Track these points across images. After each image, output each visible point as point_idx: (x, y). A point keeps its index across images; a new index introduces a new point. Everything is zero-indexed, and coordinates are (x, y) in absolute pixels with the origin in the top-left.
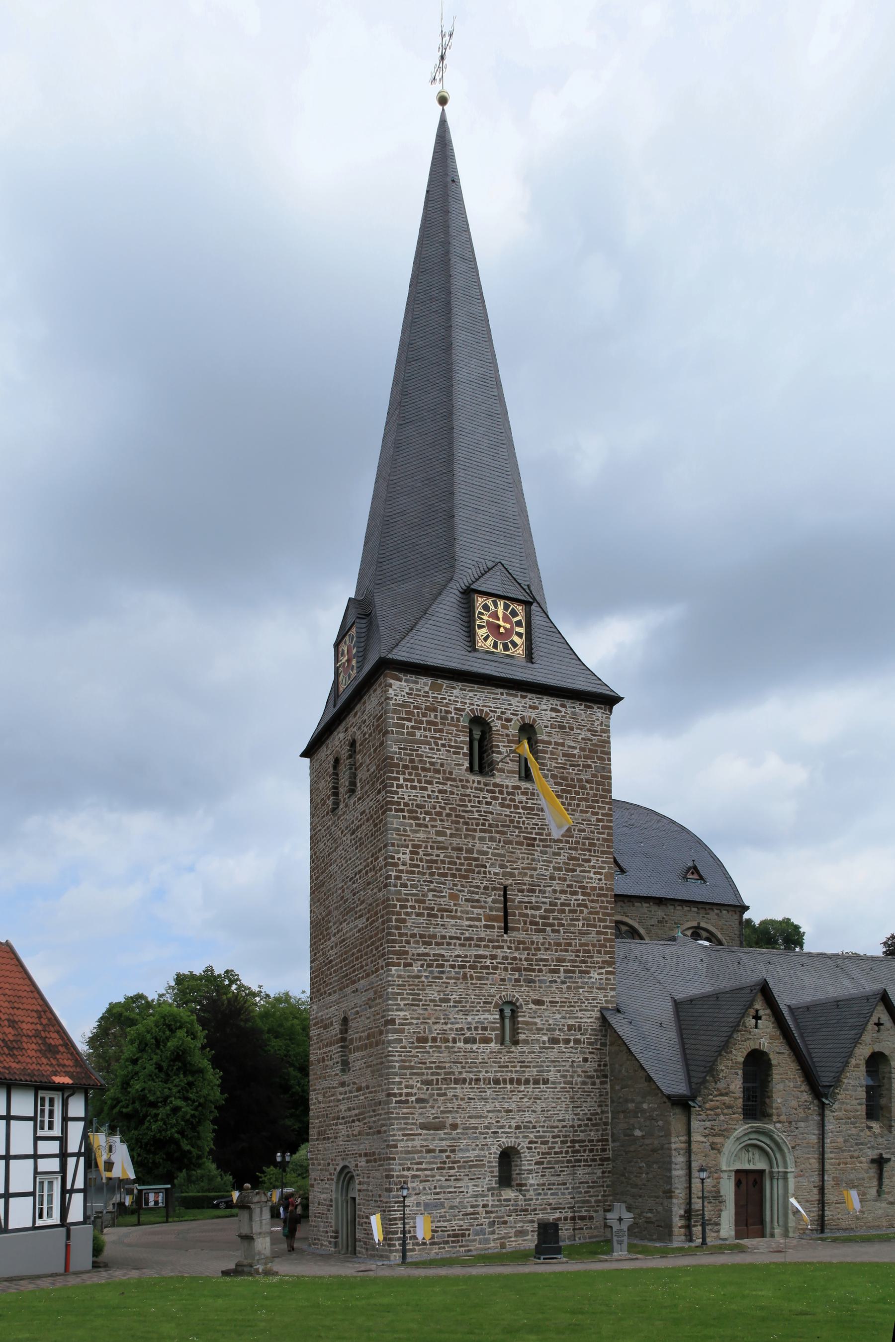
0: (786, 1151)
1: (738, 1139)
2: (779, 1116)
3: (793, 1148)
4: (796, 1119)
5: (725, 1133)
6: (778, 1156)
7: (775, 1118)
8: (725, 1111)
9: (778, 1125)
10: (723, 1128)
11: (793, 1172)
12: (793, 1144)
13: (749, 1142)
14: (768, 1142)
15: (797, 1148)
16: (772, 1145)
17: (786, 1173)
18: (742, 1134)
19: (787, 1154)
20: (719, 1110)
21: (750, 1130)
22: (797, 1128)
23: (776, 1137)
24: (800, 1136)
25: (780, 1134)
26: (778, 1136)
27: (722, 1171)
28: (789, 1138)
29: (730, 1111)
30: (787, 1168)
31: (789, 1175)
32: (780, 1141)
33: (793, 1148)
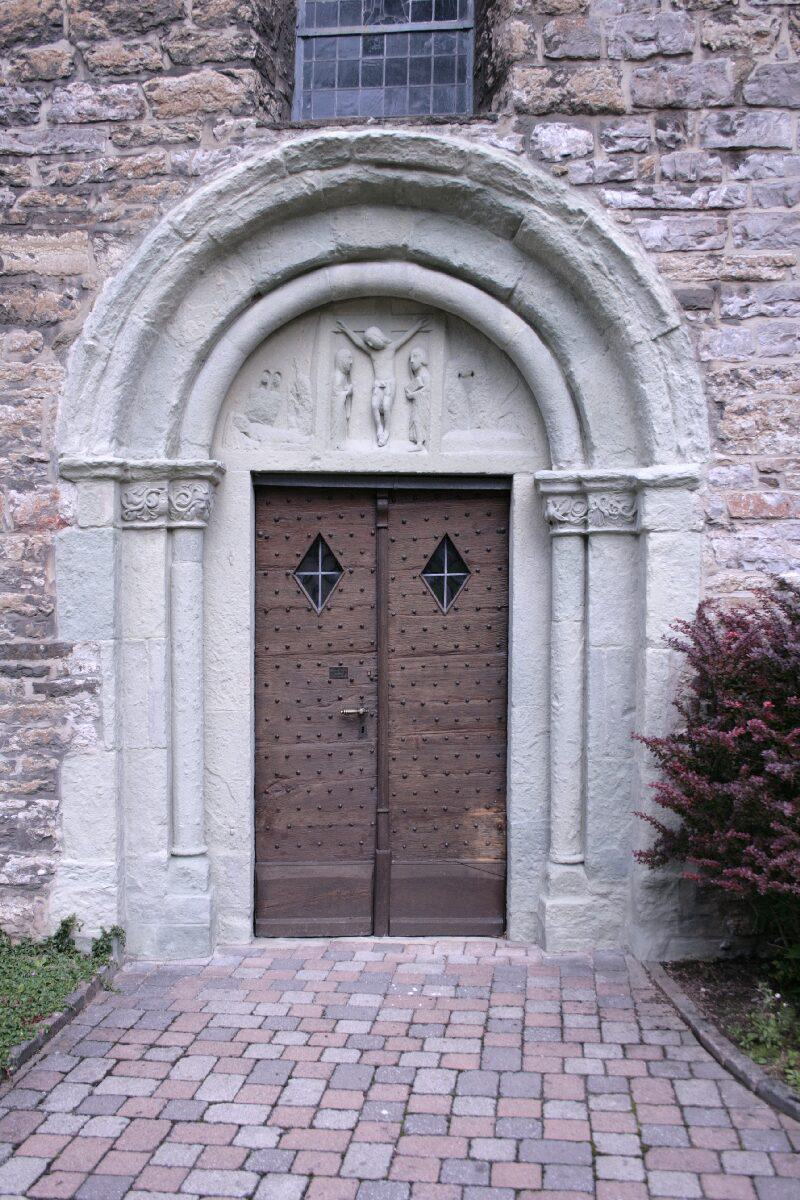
0: (635, 325)
1: (228, 249)
2: (562, 62)
3: (690, 303)
4: (723, 89)
5: (104, 204)
6: (589, 367)
7: (524, 85)
8: (111, 49)
9: (558, 137)
10: (83, 169)
11: (690, 483)
12: (694, 271)
13: (344, 276)
14: (504, 270)
15: (734, 304)
16: (538, 294)
17: (635, 490)
18: (244, 210)
19: (648, 357)
20: (62, 46)
21: (314, 180)
22: (736, 155)
23: (540, 219)
24: (758, 221)
25: (575, 201)
26: (566, 214)
27: (72, 474)
28: (656, 230)
29: (149, 51)
30: (646, 457)
31: (654, 507)
32: (582, 254)
33: (690, 303)
